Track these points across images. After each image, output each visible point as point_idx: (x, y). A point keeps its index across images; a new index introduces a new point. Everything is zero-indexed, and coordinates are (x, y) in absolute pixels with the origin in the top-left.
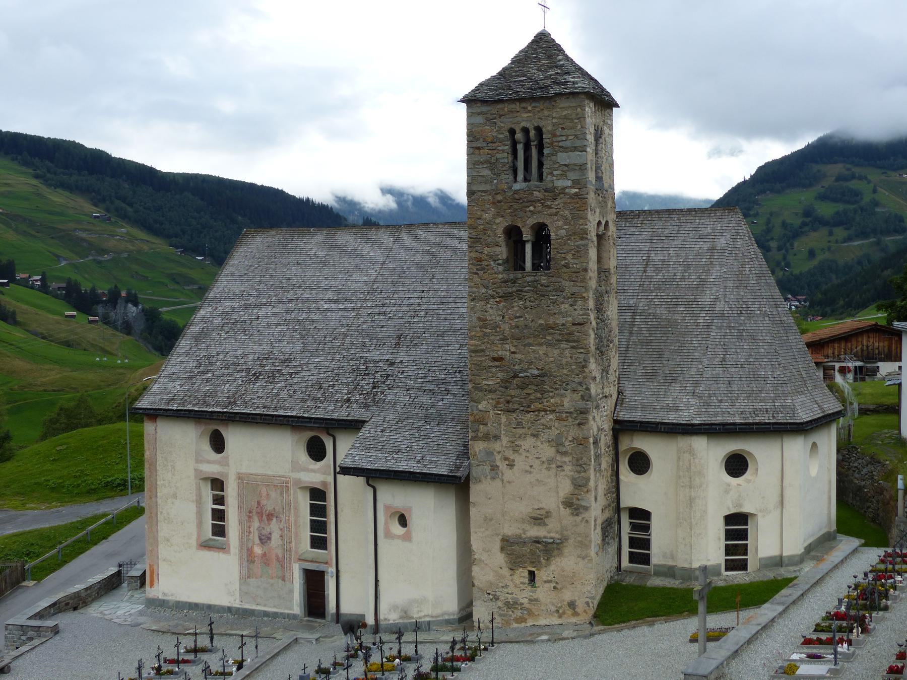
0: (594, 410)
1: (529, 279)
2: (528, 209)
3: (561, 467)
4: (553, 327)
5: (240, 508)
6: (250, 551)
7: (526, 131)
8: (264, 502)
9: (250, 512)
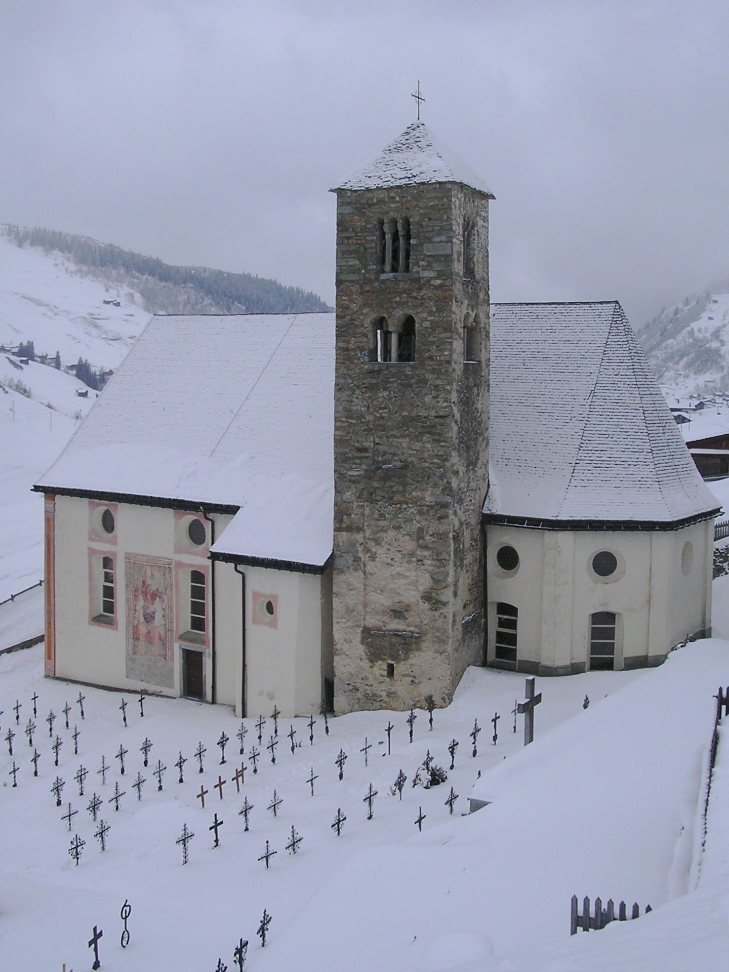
0: (456, 505)
1: (393, 370)
2: (394, 300)
3: (421, 561)
4: (417, 418)
5: (127, 586)
6: (135, 629)
7: (395, 222)
8: (149, 582)
9: (136, 591)
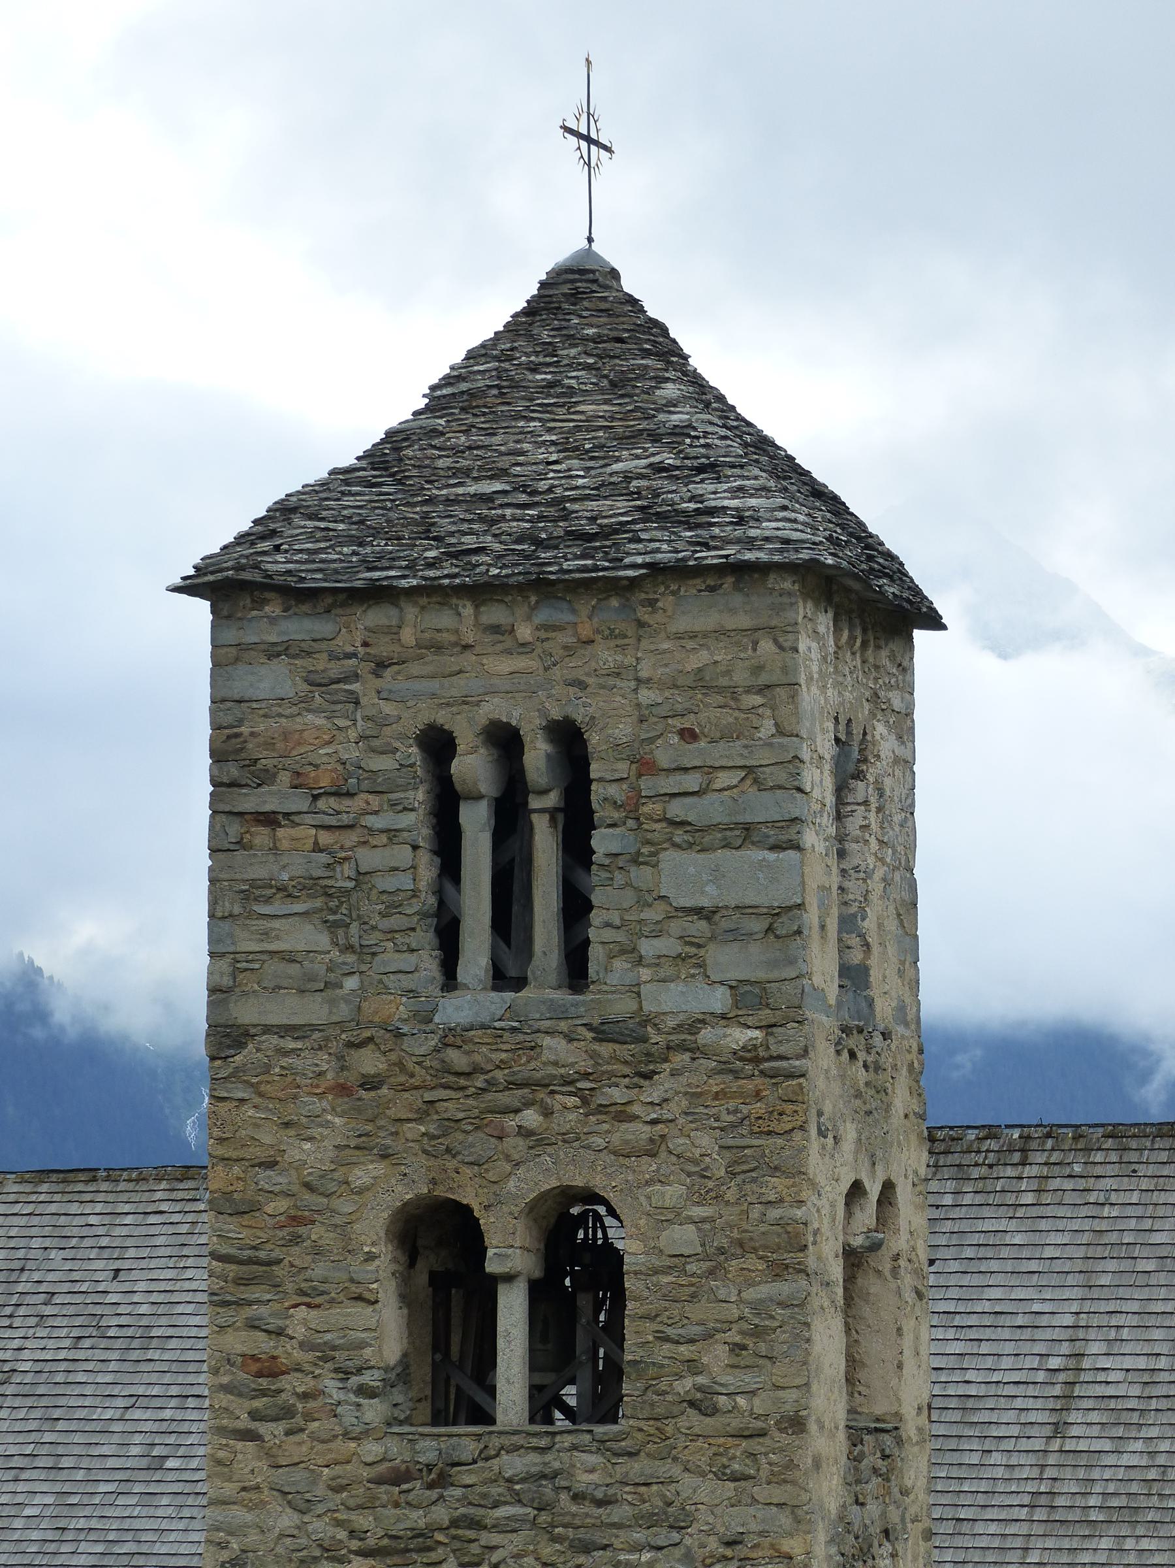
1: (515, 1464)
2: (511, 1122)
